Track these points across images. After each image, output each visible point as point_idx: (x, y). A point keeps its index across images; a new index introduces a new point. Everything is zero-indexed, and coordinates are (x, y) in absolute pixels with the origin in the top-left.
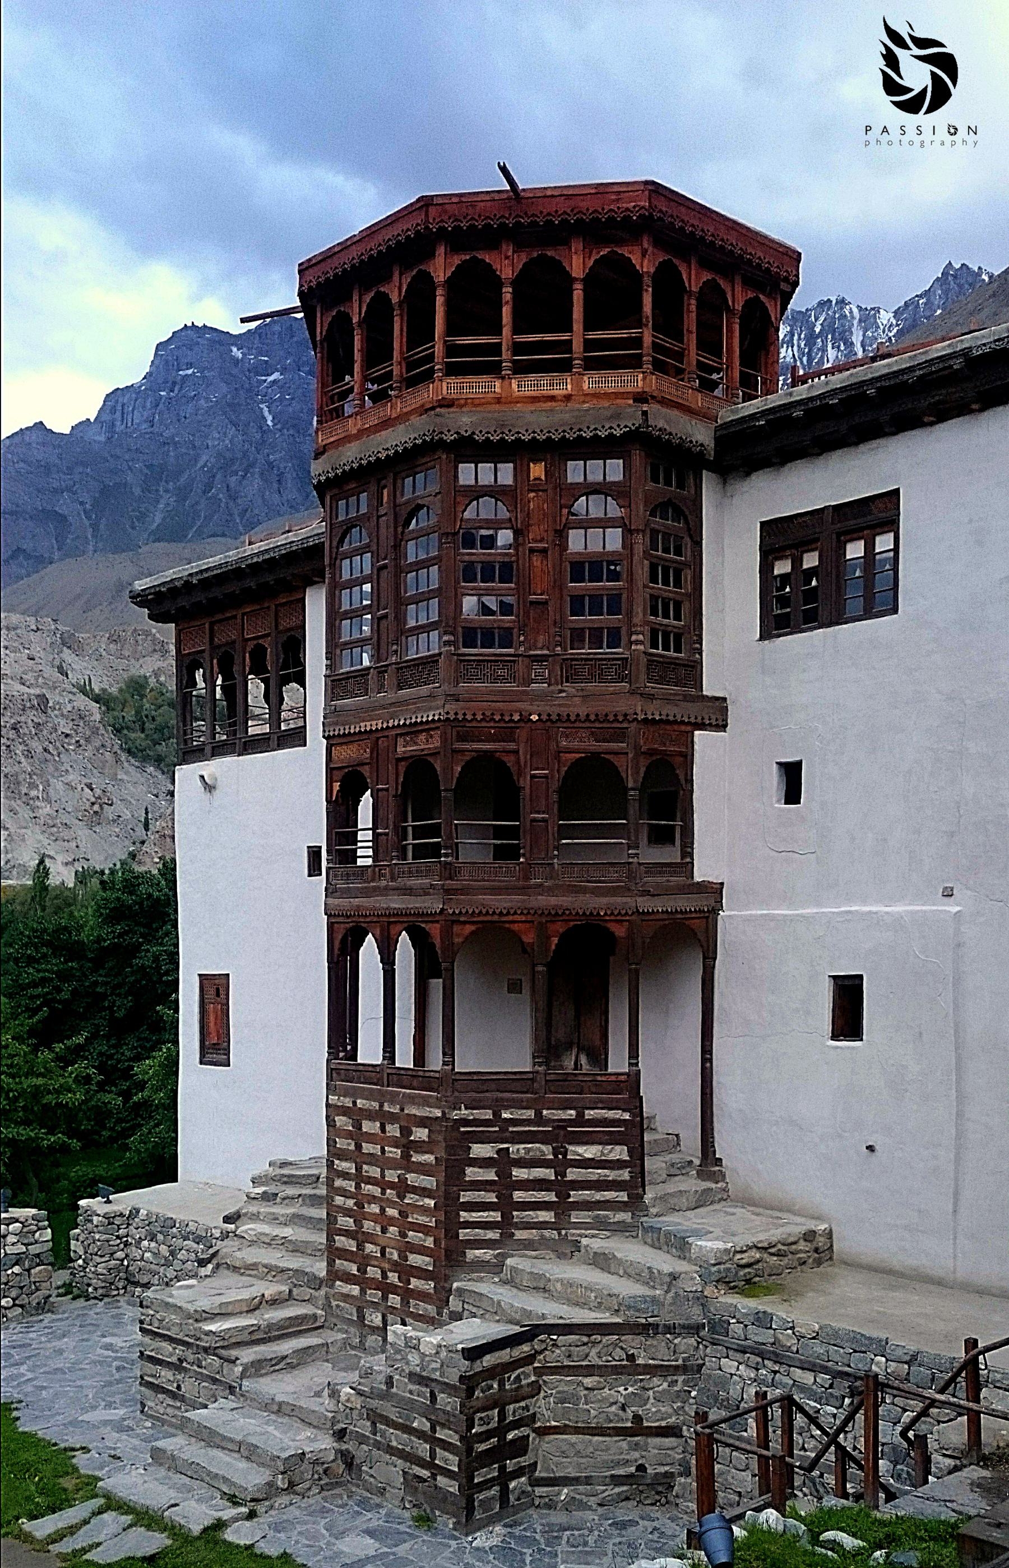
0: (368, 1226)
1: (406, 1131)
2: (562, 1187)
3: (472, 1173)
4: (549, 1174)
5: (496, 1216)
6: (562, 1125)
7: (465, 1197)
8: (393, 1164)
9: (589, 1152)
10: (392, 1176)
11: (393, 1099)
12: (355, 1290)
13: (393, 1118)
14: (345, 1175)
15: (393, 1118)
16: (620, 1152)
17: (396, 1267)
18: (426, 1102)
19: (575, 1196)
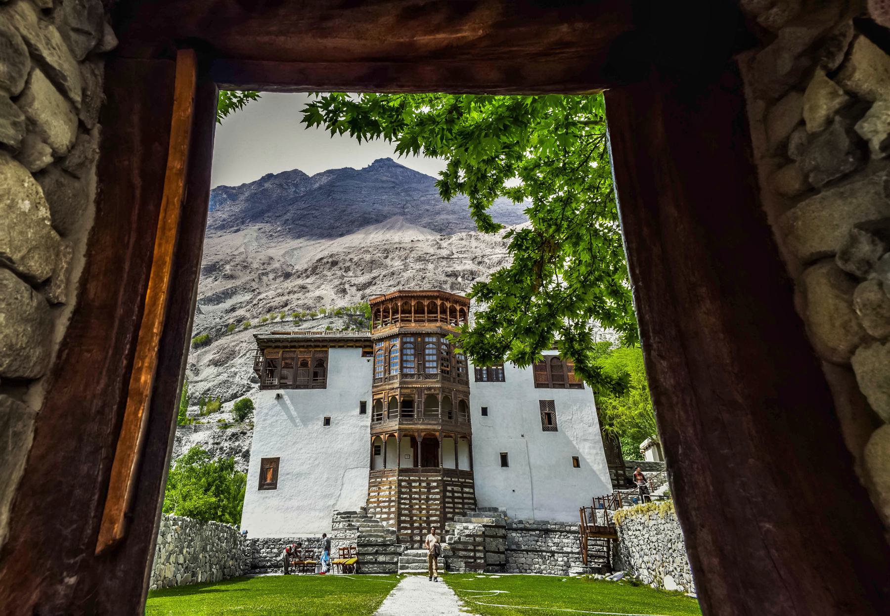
0: (414, 512)
1: (428, 484)
2: (463, 498)
3: (448, 494)
4: (460, 495)
5: (451, 505)
6: (462, 483)
7: (447, 500)
8: (424, 493)
9: (467, 490)
10: (423, 497)
11: (424, 476)
12: (409, 531)
13: (423, 481)
14: (405, 499)
15: (423, 481)
16: (471, 491)
17: (425, 522)
18: (436, 476)
19: (466, 501)
